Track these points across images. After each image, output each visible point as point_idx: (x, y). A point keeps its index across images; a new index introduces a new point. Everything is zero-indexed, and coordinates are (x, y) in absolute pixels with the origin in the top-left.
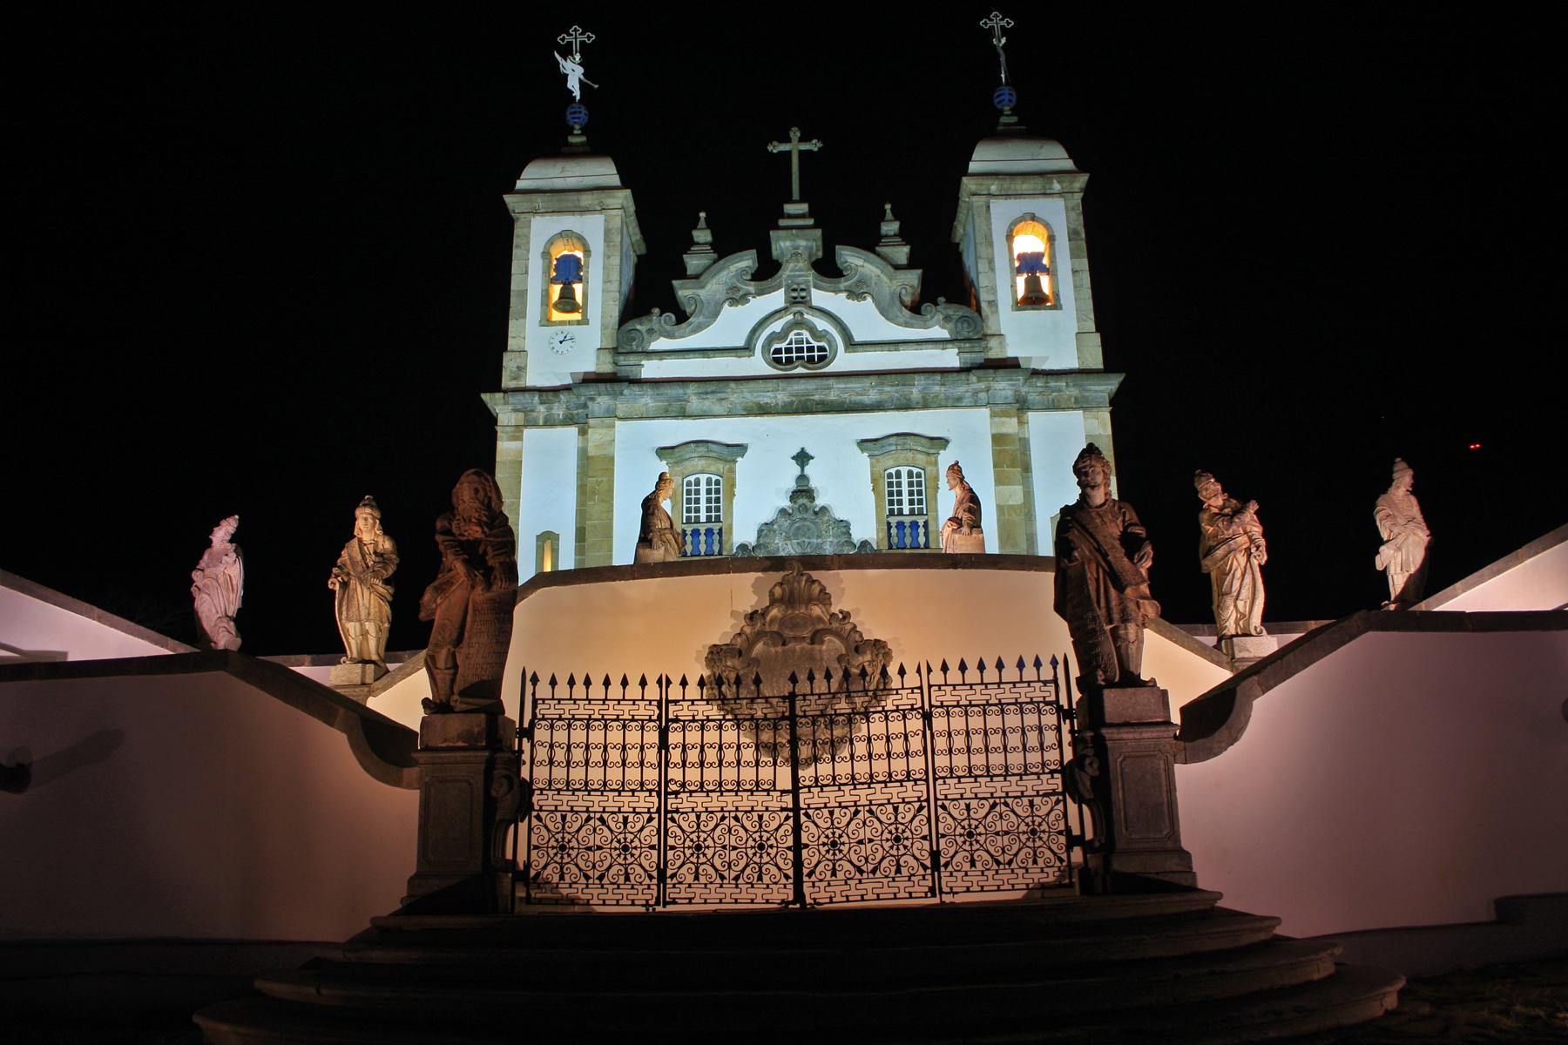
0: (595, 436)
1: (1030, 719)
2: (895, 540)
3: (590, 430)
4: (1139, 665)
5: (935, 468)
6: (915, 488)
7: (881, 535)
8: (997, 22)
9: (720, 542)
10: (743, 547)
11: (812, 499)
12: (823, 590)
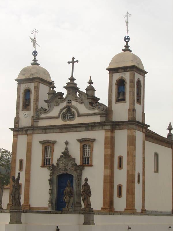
2: (84, 162)
6: (90, 149)
10: (53, 165)
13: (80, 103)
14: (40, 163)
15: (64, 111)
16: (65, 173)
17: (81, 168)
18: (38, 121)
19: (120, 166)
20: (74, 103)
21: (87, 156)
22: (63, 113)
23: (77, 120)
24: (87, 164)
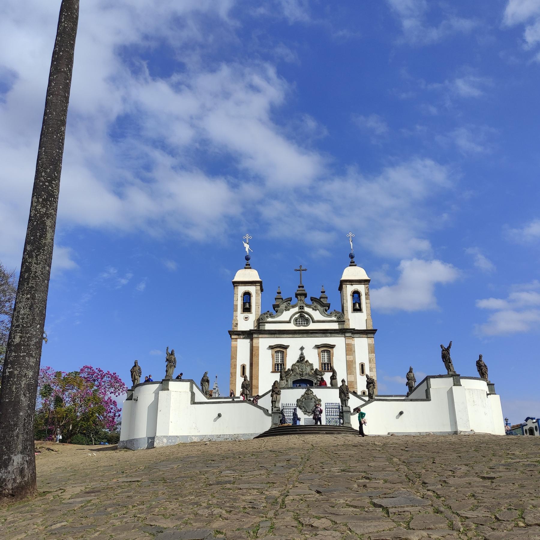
0: (255, 341)
1: (336, 410)
2: (324, 368)
3: (254, 340)
4: (348, 404)
5: (332, 351)
7: (320, 367)
11: (304, 358)
12: (312, 391)
13: (313, 309)
14: (270, 368)
17: (323, 373)
18: (265, 325)
19: (363, 371)
20: (306, 309)
21: (326, 362)
22: (296, 318)
23: (312, 326)
24: (326, 370)
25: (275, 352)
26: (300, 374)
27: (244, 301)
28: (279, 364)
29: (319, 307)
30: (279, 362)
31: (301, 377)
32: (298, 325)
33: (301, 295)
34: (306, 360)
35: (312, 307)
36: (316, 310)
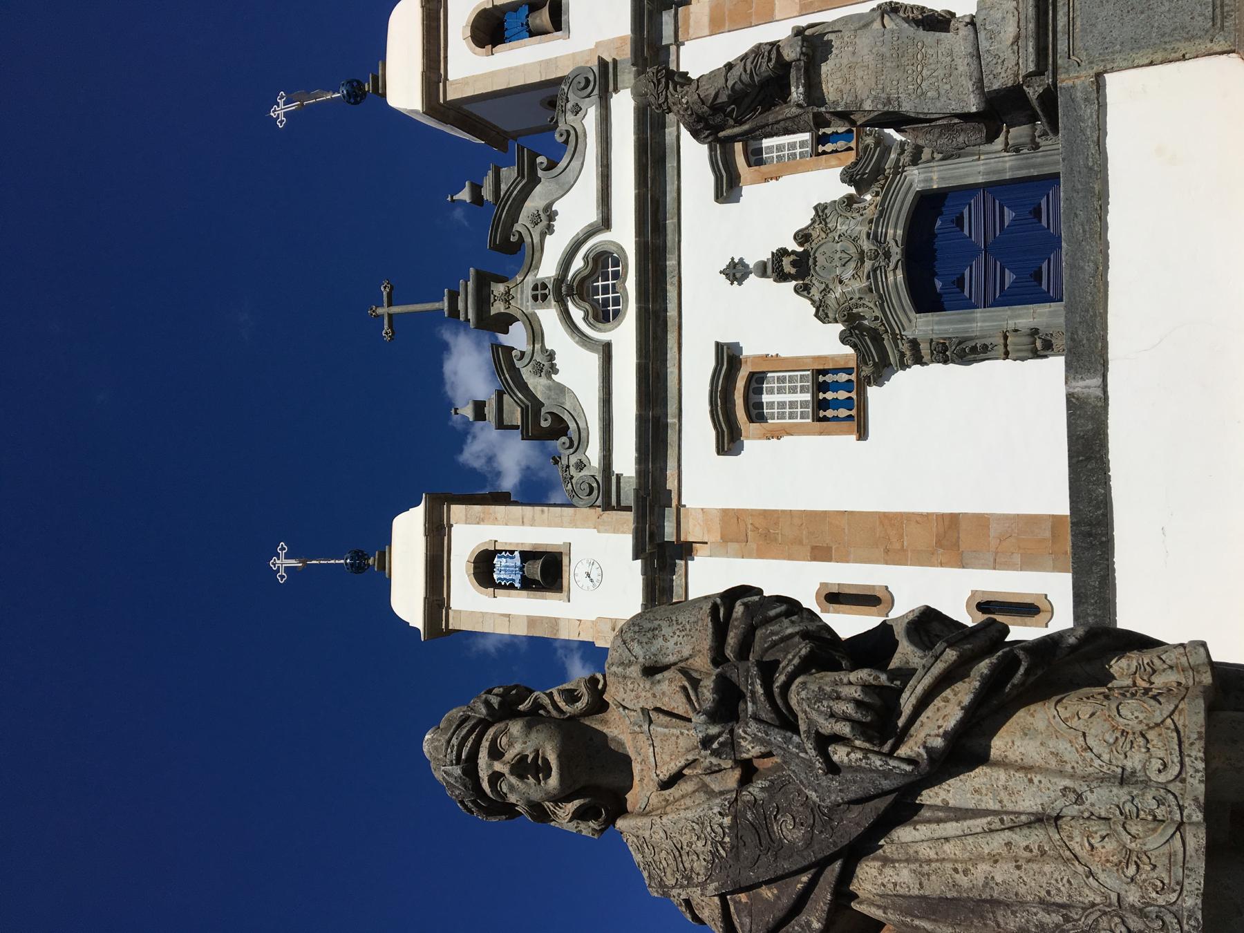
7: (833, 163)
8: (280, 111)
9: (836, 371)
11: (783, 252)
13: (550, 229)
15: (577, 314)
16: (898, 250)
18: (619, 477)
20: (548, 268)
22: (584, 319)
25: (751, 420)
26: (875, 270)
27: (517, 585)
28: (814, 396)
29: (534, 203)
30: (807, 397)
31: (892, 266)
32: (620, 307)
33: (483, 301)
34: (793, 246)
35: (536, 240)
36: (552, 216)
